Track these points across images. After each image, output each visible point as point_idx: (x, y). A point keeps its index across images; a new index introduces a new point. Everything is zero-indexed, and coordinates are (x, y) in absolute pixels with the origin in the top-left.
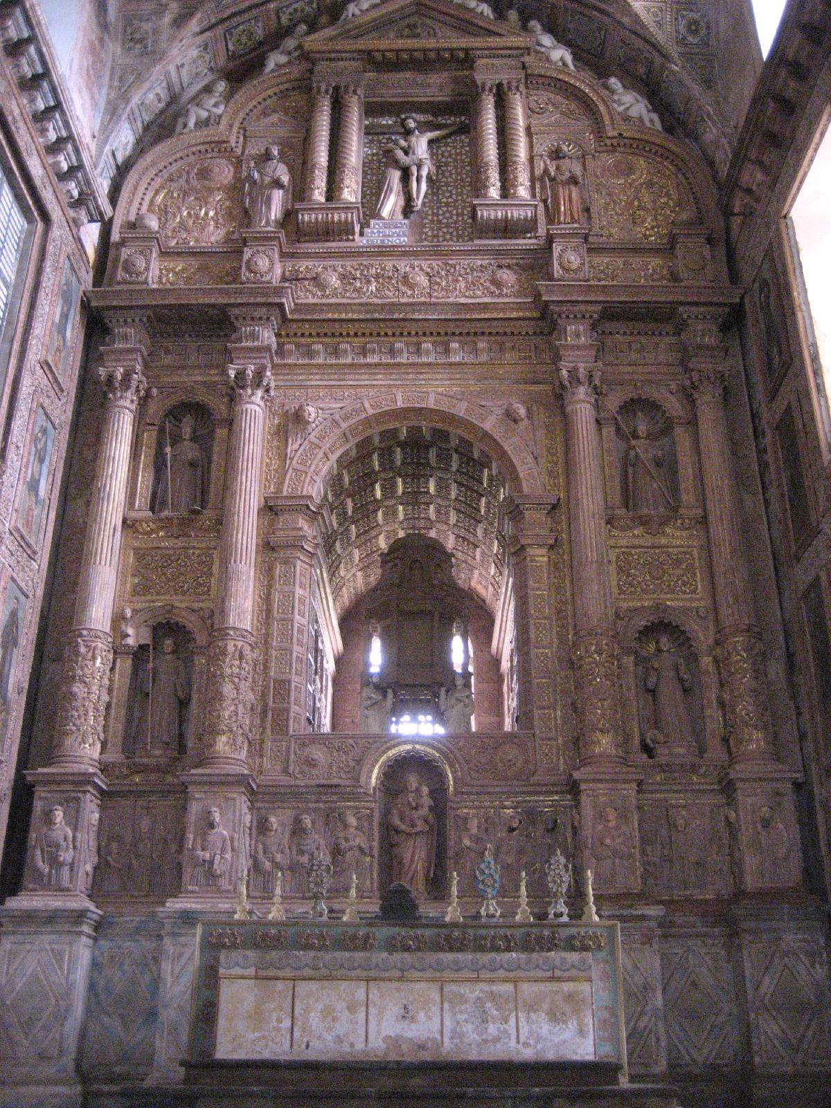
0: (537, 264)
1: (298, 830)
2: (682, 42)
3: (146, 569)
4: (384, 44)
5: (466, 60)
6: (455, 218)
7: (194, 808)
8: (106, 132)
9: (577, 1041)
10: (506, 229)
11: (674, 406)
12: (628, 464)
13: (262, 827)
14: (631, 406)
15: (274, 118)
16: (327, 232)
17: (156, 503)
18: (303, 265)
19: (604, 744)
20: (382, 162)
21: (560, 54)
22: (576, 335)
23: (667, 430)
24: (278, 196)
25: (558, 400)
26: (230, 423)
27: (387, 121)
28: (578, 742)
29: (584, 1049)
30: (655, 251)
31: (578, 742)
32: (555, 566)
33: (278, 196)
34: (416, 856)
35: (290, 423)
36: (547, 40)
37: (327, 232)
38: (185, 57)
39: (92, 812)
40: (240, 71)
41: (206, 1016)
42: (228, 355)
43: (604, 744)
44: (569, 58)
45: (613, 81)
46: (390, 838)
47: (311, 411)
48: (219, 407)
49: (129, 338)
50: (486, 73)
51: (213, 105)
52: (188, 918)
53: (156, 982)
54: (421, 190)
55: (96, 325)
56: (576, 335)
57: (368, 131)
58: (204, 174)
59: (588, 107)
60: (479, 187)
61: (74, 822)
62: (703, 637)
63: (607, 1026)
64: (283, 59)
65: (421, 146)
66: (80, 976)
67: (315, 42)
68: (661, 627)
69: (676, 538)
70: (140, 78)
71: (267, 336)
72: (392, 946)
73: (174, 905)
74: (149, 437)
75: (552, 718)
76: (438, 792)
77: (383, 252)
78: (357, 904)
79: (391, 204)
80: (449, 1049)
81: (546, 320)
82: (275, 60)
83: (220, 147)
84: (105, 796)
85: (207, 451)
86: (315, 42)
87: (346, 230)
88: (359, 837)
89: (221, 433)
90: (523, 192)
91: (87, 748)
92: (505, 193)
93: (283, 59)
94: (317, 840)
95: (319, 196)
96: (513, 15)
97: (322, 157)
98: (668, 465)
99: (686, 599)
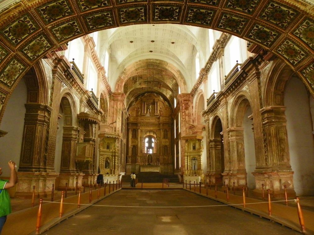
0: (159, 118)
1: (143, 159)
2: (171, 100)
3: (132, 142)
4: (148, 98)
5: (154, 99)
6: (153, 114)
7: (137, 158)
8: (127, 107)
9: (158, 171)
10: (157, 116)
11: (168, 130)
12: (164, 134)
13: (141, 159)
14: (165, 130)
15: (139, 104)
16: (144, 116)
17: (133, 137)
18: (142, 118)
19: (161, 154)
20: (148, 108)
21: (162, 99)
22: (161, 125)
23: (167, 131)
24: (140, 112)
25: (160, 130)
26: (138, 131)
27: (148, 103)
28: (160, 154)
29: (158, 171)
30: (168, 117)
31: (160, 154)
32: (159, 142)
33: (140, 112)
34: (150, 160)
35: (142, 131)
36: (161, 97)
37: (144, 116)
38: (132, 99)
39: (131, 158)
40: (136, 99)
41: (140, 169)
42: (137, 127)
43: (161, 154)
44: (162, 98)
45: (166, 102)
46: (148, 160)
47: (143, 131)
48: (136, 129)
49: (130, 125)
50: (156, 101)
51: (134, 103)
52: (137, 164)
53: (135, 168)
54: (151, 111)
55: (128, 124)
56: (161, 125)
57: (146, 104)
58: (134, 109)
59: (164, 104)
60: (155, 112)
61: (130, 159)
62: (168, 147)
63: (160, 170)
64: (140, 98)
65: (151, 107)
66: (131, 168)
67: (142, 98)
68: (166, 146)
69: (167, 140)
70: (129, 102)
71: (140, 125)
72: (149, 166)
73: (137, 164)
74: (132, 132)
75: (158, 152)
76: (151, 156)
77: (148, 117)
78: (147, 163)
79: (148, 112)
80: (152, 171)
81: (160, 124)
82: (139, 99)
83: (135, 107)
84: (131, 157)
85: (136, 133)
86: (142, 98)
87: (145, 116)
88: (147, 159)
89: (137, 132)
90: (158, 112)
91: (130, 154)
92: (157, 113)
93: (140, 98)
94: (144, 160)
95: (143, 112)
96: (158, 95)
97: (143, 109)
98: (167, 135)
99: (167, 144)
